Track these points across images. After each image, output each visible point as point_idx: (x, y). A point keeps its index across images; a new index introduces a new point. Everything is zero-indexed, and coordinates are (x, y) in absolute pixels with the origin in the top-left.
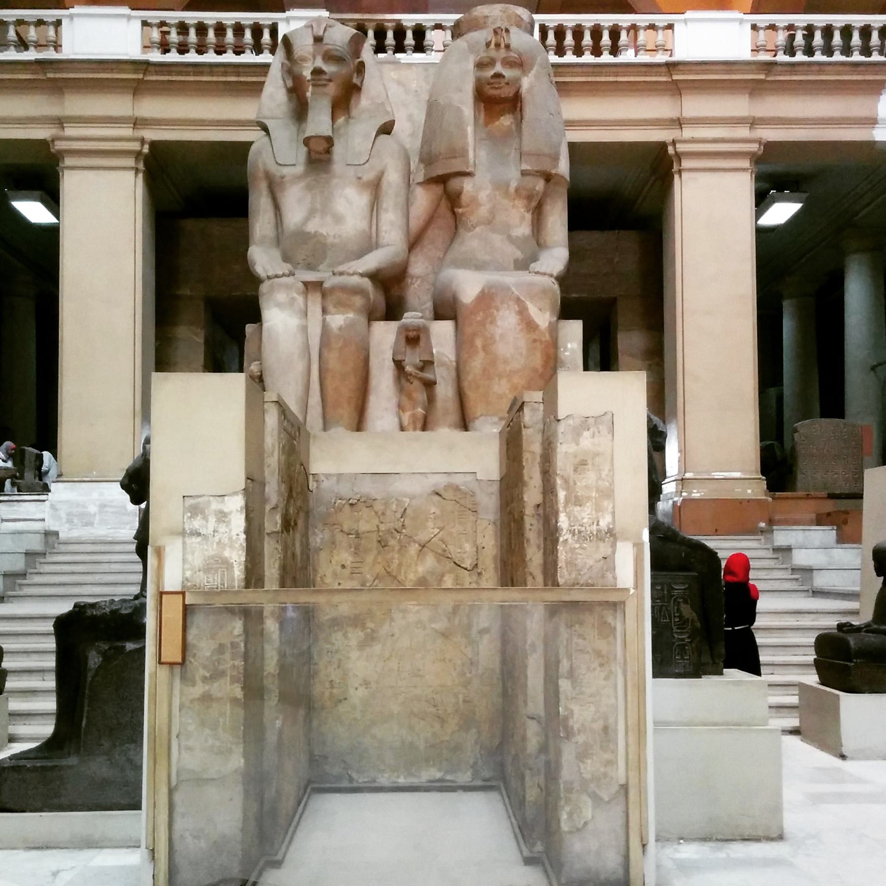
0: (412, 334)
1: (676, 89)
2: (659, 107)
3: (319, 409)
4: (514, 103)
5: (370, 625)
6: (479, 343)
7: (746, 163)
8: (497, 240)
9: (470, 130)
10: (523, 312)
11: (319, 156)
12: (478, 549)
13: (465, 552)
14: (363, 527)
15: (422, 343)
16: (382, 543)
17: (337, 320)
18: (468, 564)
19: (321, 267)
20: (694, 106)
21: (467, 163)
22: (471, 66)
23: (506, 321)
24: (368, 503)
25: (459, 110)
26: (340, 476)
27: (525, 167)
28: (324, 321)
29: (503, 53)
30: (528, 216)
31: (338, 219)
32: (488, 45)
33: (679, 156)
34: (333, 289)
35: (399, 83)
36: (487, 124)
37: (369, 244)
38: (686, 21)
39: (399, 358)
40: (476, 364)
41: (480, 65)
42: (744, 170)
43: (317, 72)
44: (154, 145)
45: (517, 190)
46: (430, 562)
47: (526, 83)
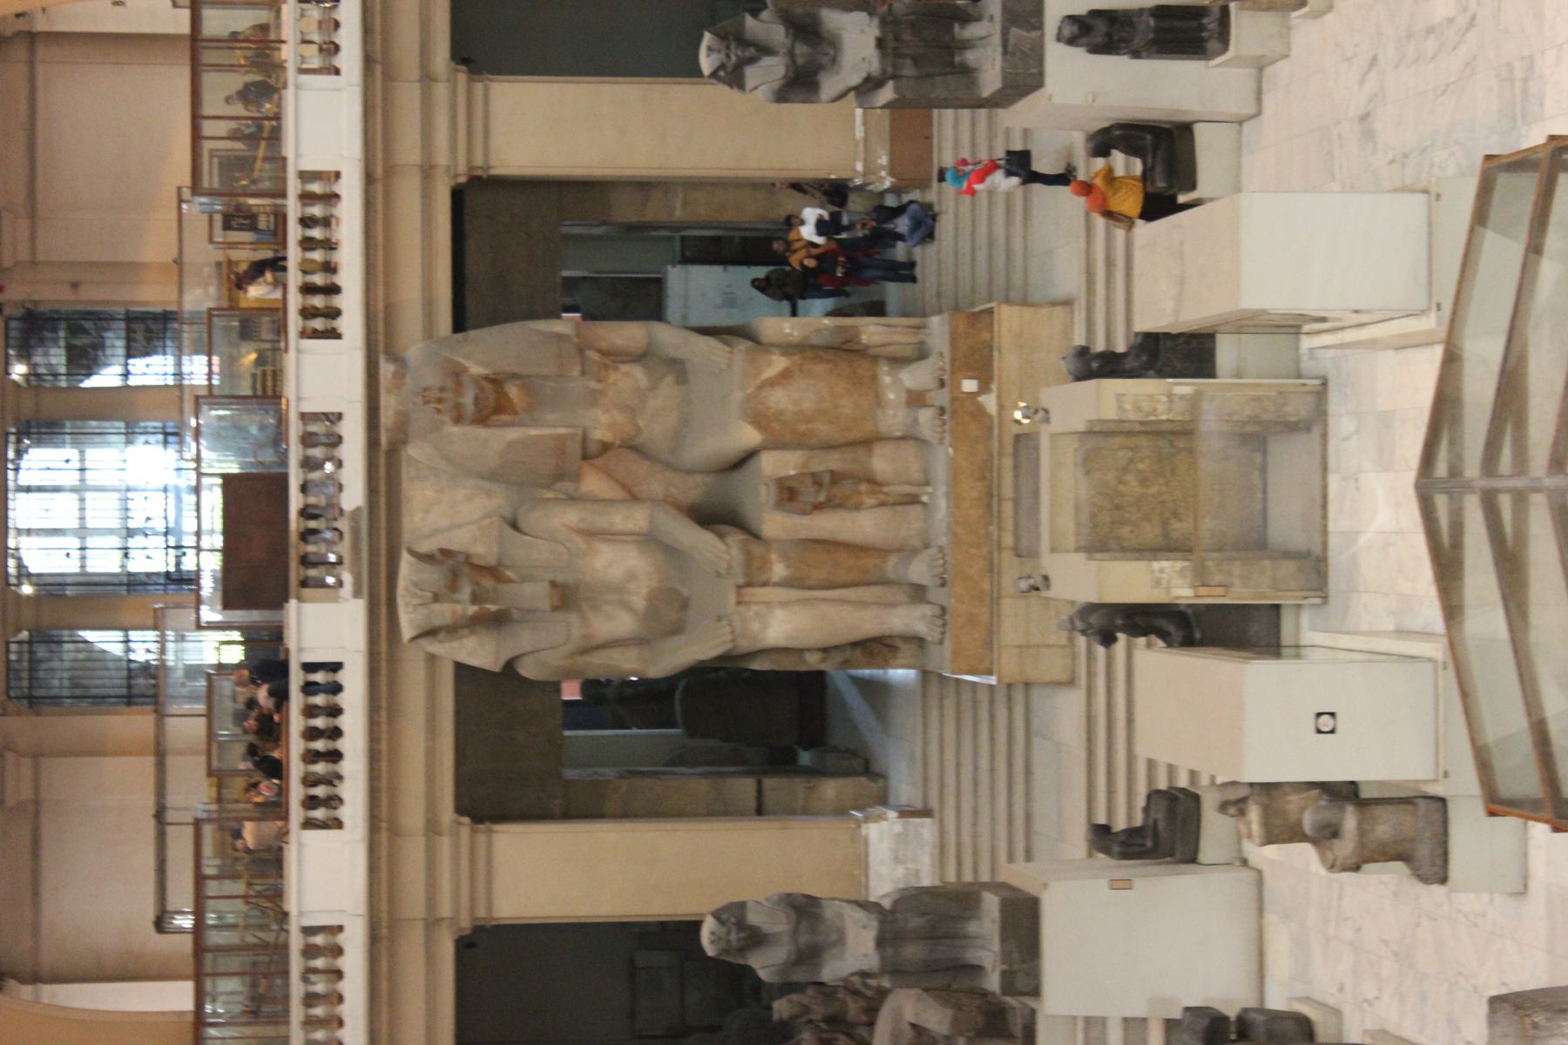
0: (786, 496)
1: (390, 171)
2: (408, 192)
3: (861, 590)
4: (496, 381)
5: (1167, 515)
6: (803, 427)
7: (479, 87)
8: (654, 403)
9: (533, 432)
10: (772, 383)
11: (566, 597)
12: (1123, 448)
13: (1124, 455)
14: (1109, 519)
15: (793, 484)
16: (1118, 507)
17: (779, 570)
18: (1129, 454)
19: (685, 592)
20: (409, 151)
21: (572, 436)
22: (455, 430)
23: (779, 399)
24: (1093, 516)
25: (511, 445)
26: (1077, 534)
27: (576, 372)
28: (777, 585)
29: (448, 395)
30: (624, 368)
31: (631, 576)
32: (439, 411)
33: (471, 168)
34: (747, 575)
35: (427, 512)
36: (515, 413)
37: (649, 540)
38: (298, 155)
39: (809, 507)
40: (823, 429)
41: (458, 419)
42: (486, 91)
43: (475, 599)
44: (460, 810)
45: (600, 381)
46: (1130, 478)
47: (476, 369)
